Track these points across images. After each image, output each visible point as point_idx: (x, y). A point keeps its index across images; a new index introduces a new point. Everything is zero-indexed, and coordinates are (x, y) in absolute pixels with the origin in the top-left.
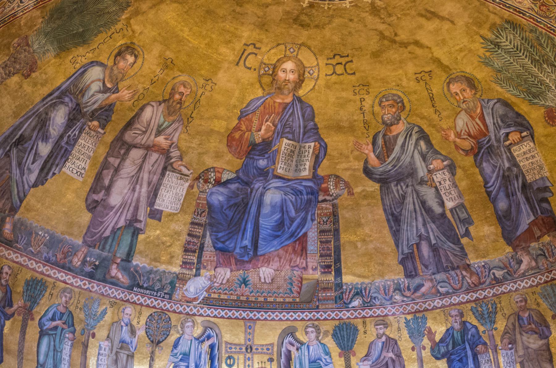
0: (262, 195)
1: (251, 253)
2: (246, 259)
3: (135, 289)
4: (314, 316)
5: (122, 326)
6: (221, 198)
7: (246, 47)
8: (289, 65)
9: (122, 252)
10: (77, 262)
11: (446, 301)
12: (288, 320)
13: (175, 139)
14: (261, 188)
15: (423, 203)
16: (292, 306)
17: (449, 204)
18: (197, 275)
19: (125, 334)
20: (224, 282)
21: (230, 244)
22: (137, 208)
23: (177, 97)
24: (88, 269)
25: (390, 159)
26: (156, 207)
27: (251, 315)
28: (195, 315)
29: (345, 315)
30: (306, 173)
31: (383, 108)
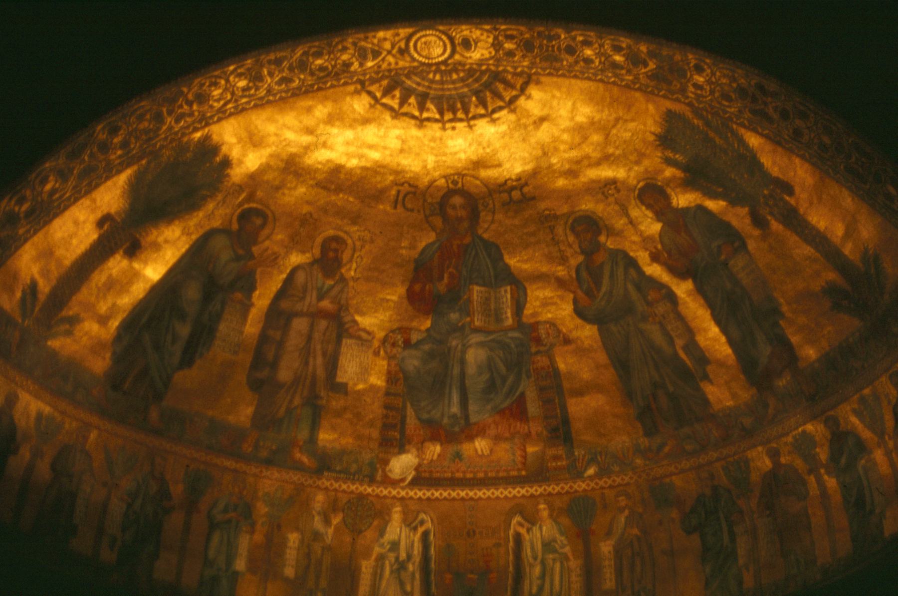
0: (464, 352)
1: (462, 422)
2: (457, 429)
3: (326, 474)
4: (545, 490)
5: (314, 517)
6: (416, 363)
7: (400, 188)
8: (457, 200)
9: (303, 434)
10: (247, 448)
12: (515, 497)
13: (343, 302)
14: (460, 346)
17: (679, 343)
18: (402, 450)
19: (318, 523)
20: (435, 457)
21: (436, 414)
22: (314, 383)
23: (331, 254)
24: (264, 454)
25: (601, 294)
26: (339, 379)
27: (471, 494)
28: (403, 499)
29: (580, 486)
30: (509, 322)
31: (577, 235)
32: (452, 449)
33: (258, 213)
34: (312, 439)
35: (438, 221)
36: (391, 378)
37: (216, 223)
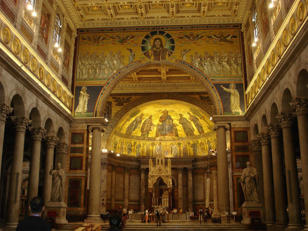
8: (166, 111)
9: (147, 136)
11: (192, 140)
15: (188, 127)
16: (172, 140)
18: (158, 137)
24: (142, 139)
32: (164, 137)
33: (143, 114)
34: (148, 137)
35: (163, 113)
36: (157, 129)
37: (138, 116)
